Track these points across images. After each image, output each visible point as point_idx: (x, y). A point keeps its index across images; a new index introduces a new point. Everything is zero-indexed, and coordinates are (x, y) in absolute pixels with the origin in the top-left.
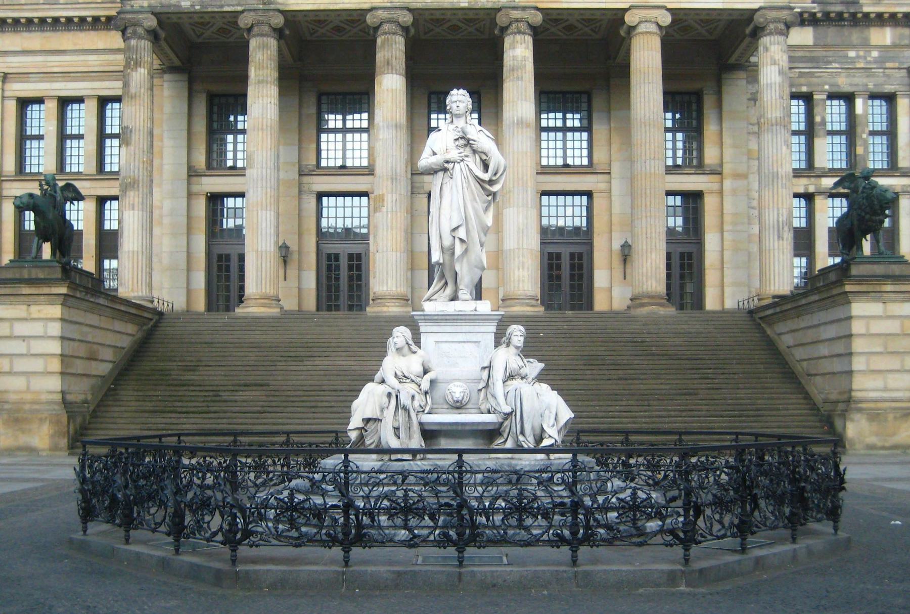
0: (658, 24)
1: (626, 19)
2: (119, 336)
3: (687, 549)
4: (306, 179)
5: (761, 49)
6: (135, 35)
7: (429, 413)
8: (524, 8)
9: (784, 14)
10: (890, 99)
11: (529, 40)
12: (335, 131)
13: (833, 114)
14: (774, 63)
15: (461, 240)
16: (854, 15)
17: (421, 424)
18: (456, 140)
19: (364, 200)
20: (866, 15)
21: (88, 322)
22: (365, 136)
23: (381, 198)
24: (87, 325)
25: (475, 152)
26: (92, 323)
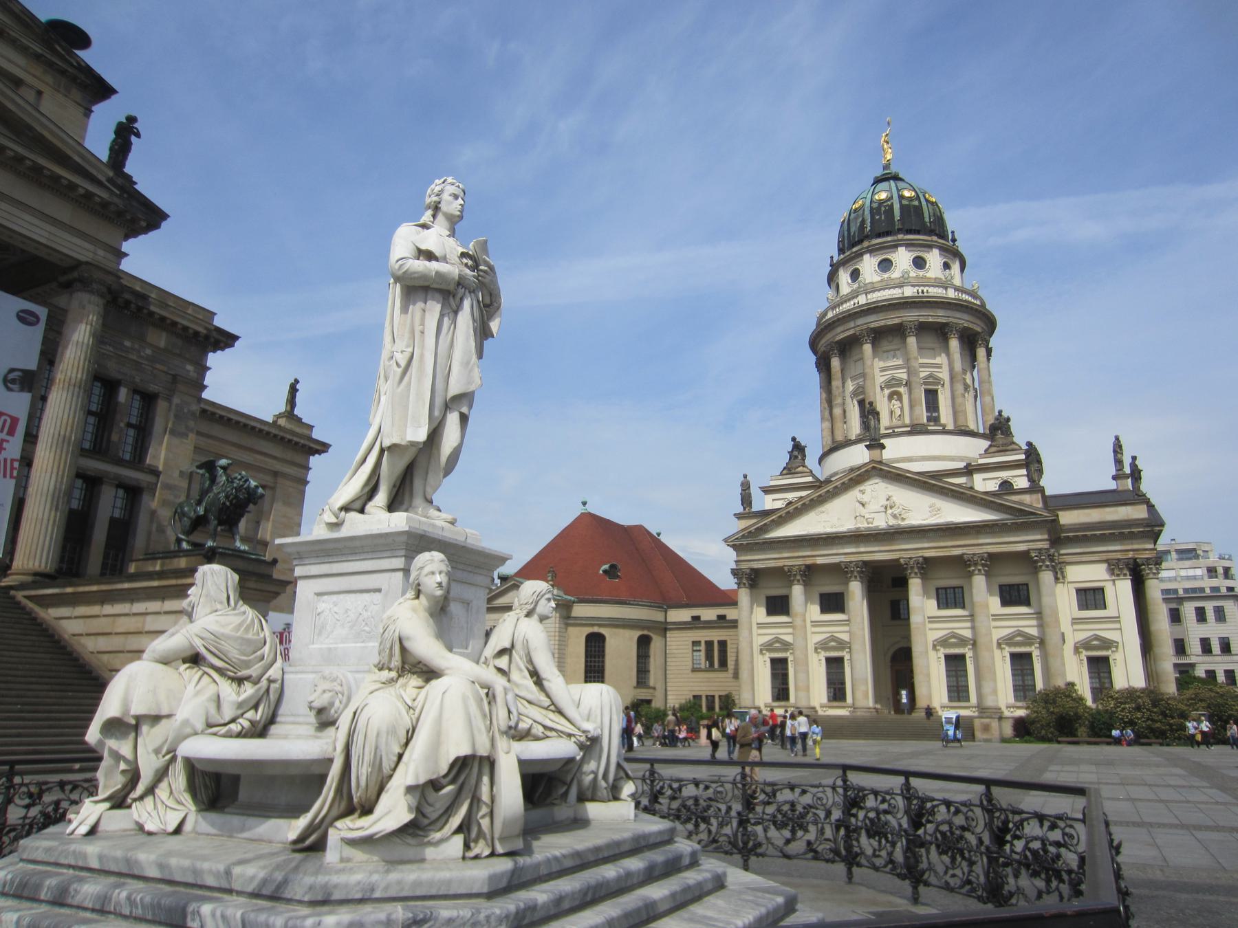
10: (149, 400)
16: (140, 309)
18: (463, 255)
20: (151, 314)
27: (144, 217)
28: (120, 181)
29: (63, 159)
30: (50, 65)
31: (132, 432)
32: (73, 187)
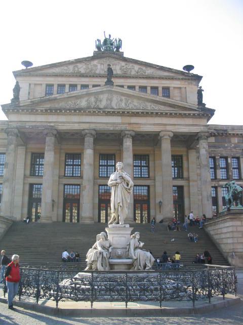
0: (169, 136)
1: (160, 135)
3: (194, 302)
4: (61, 180)
5: (200, 144)
6: (11, 135)
8: (129, 131)
9: (207, 134)
10: (238, 158)
11: (131, 140)
12: (70, 165)
13: (222, 163)
14: (204, 148)
15: (121, 206)
16: (226, 134)
17: (109, 262)
19: (79, 186)
20: (230, 134)
22: (79, 167)
23: (85, 187)
25: (124, 180)
27: (210, 113)
28: (200, 107)
29: (185, 108)
30: (185, 79)
31: (235, 170)
32: (189, 114)
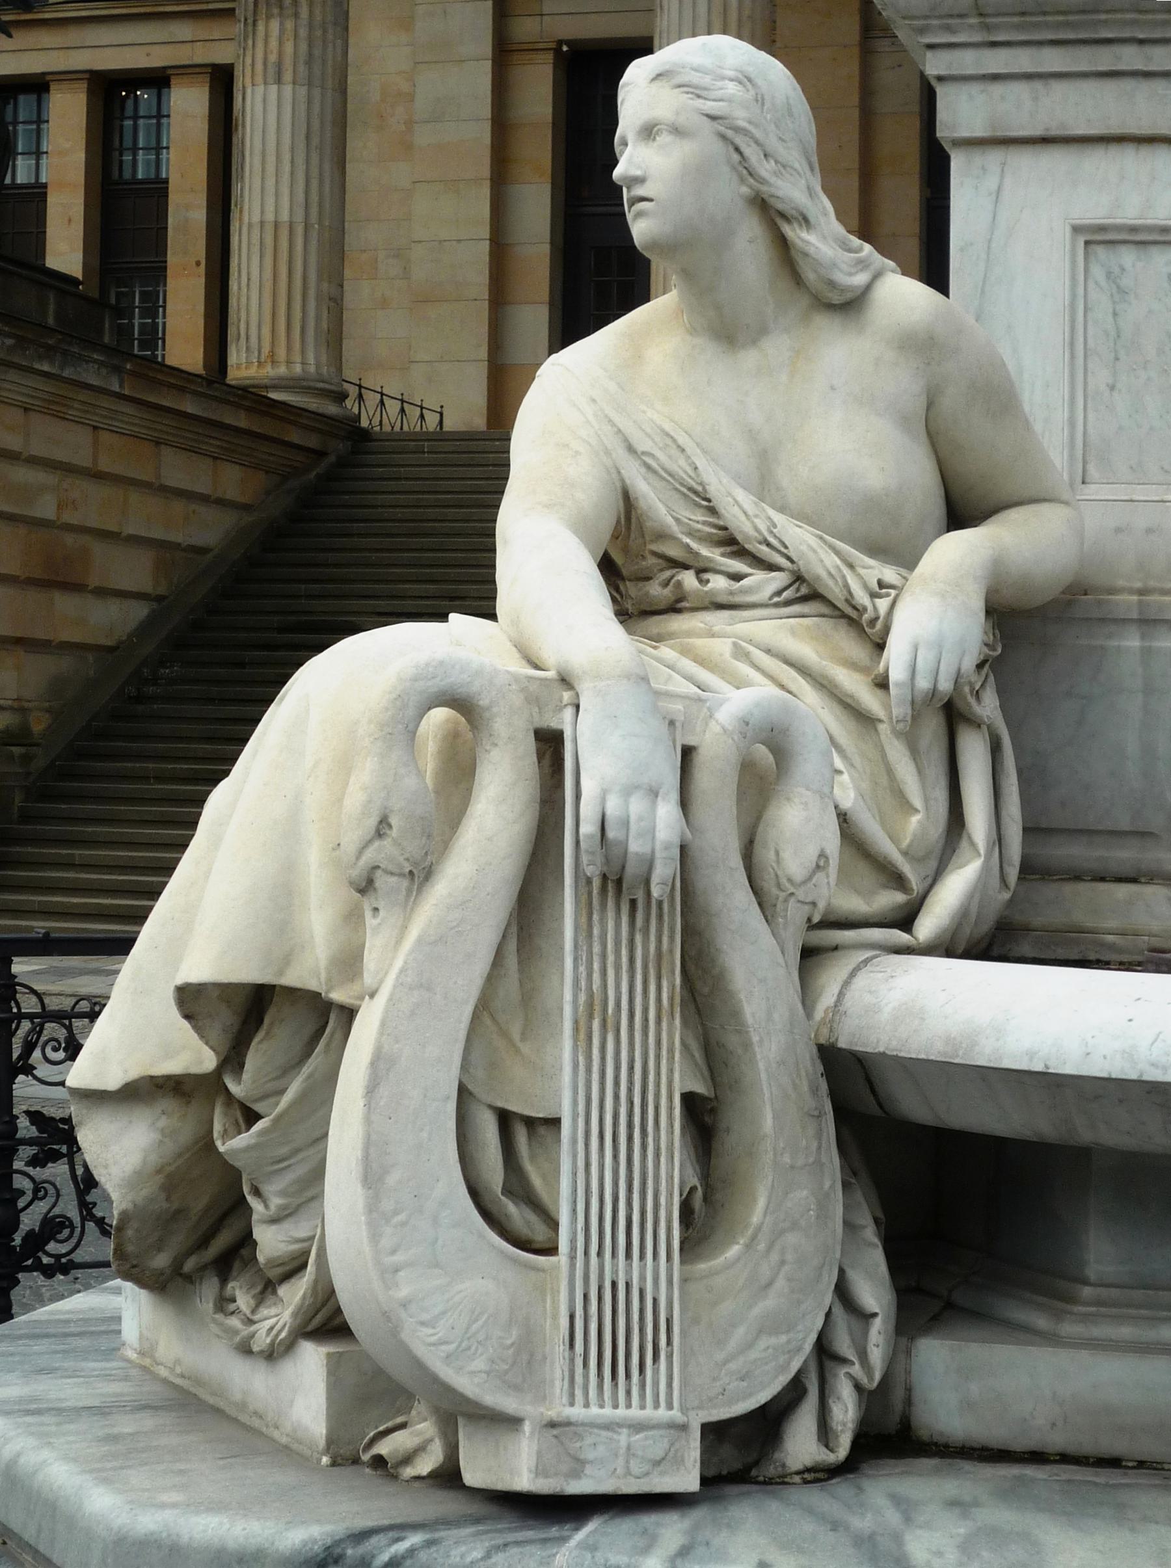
2: (178, 507)
7: (993, 938)
21: (38, 449)
24: (34, 461)
26: (60, 455)
